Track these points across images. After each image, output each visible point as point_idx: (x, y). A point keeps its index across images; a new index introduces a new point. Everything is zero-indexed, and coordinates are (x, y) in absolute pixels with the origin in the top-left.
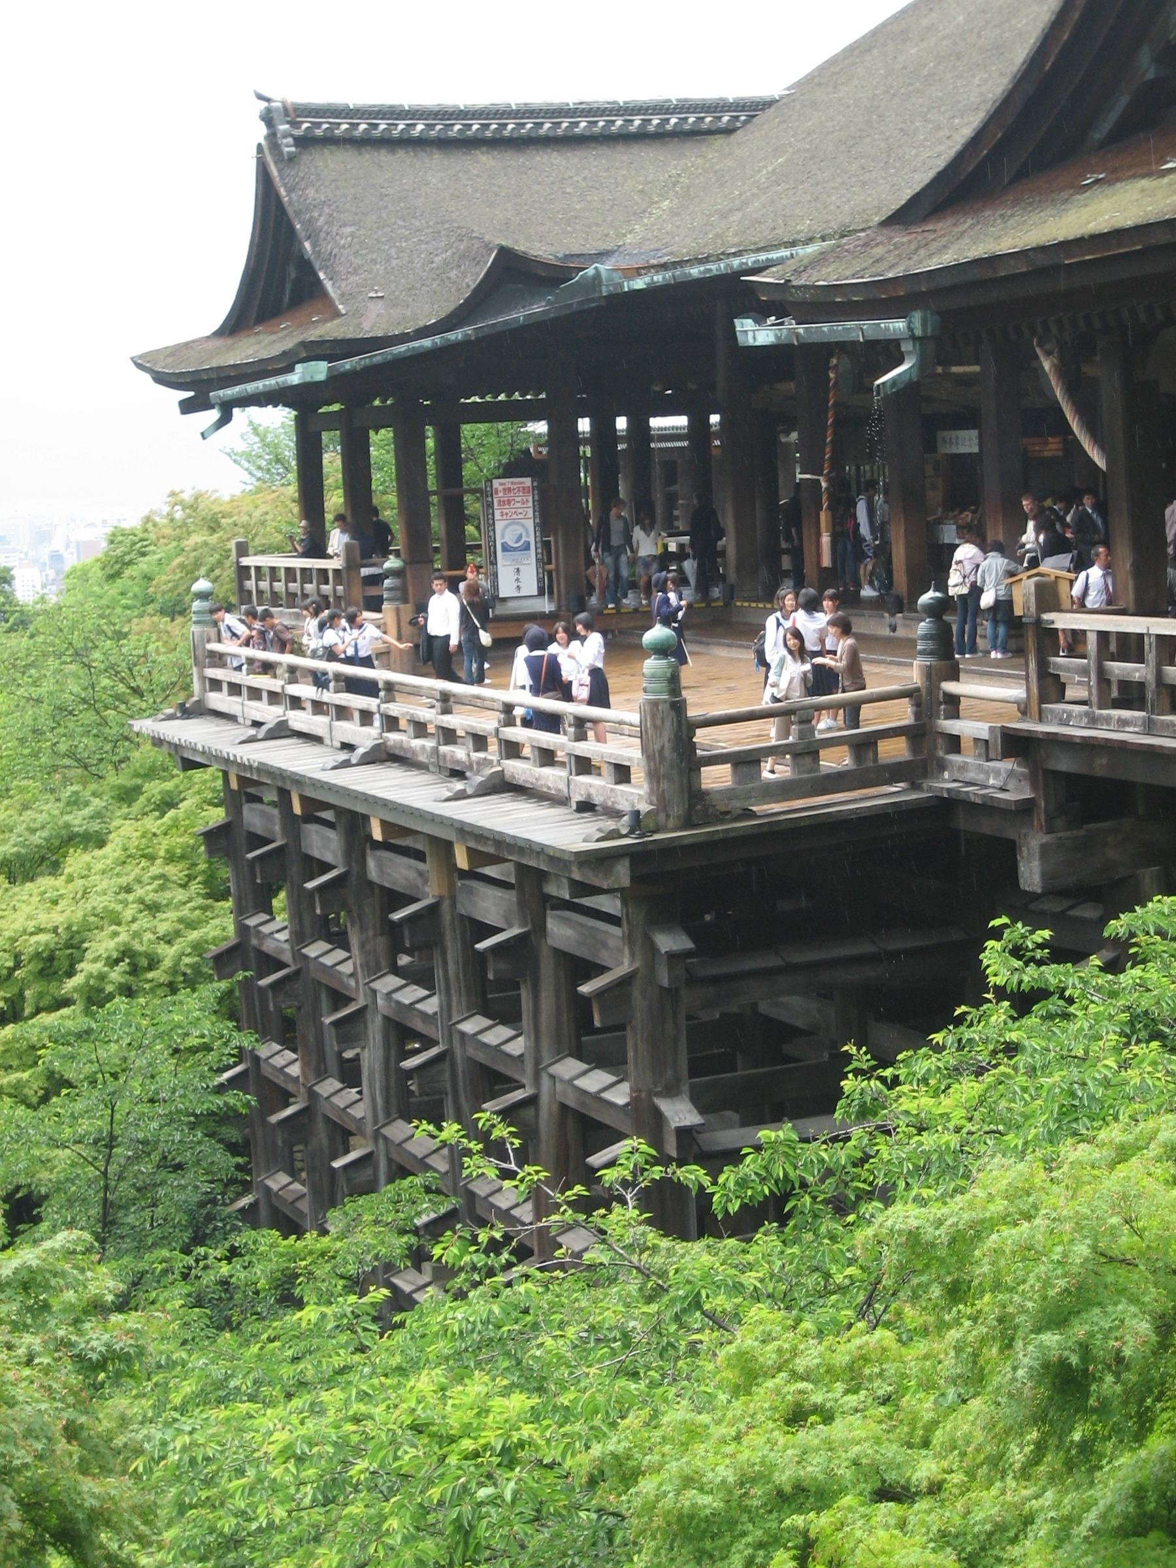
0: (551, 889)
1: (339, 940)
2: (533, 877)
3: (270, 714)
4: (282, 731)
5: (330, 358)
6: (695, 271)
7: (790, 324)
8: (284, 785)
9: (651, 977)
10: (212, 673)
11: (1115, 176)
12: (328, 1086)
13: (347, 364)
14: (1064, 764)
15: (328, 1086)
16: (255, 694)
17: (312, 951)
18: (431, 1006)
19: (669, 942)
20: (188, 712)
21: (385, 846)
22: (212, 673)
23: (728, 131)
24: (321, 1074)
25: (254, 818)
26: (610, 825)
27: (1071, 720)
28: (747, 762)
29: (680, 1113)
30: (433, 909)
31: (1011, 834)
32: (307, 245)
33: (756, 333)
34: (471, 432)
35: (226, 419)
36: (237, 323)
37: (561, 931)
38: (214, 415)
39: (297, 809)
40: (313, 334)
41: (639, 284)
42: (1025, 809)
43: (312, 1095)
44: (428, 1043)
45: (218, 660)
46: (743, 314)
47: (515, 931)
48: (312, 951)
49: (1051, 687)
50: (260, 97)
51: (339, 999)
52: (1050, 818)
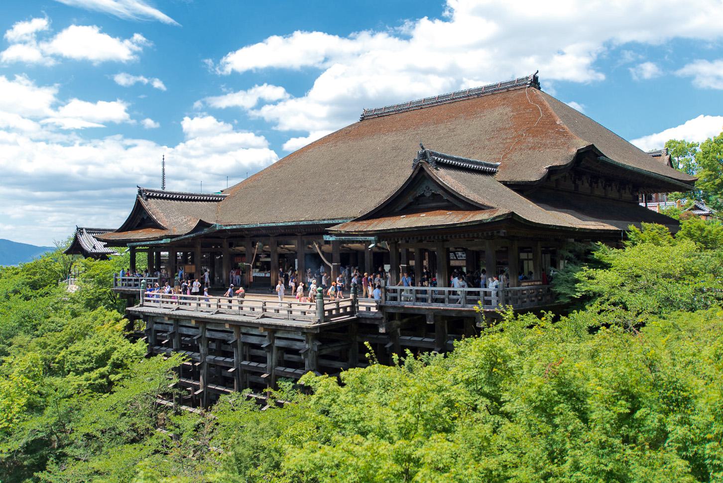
0: (278, 335)
3: (175, 306)
4: (178, 309)
5: (171, 238)
13: (174, 240)
14: (391, 311)
23: (221, 200)
28: (330, 311)
30: (236, 341)
31: (377, 323)
32: (154, 216)
33: (327, 238)
37: (278, 343)
41: (228, 228)
42: (382, 318)
45: (148, 296)
50: (138, 187)
52: (386, 319)
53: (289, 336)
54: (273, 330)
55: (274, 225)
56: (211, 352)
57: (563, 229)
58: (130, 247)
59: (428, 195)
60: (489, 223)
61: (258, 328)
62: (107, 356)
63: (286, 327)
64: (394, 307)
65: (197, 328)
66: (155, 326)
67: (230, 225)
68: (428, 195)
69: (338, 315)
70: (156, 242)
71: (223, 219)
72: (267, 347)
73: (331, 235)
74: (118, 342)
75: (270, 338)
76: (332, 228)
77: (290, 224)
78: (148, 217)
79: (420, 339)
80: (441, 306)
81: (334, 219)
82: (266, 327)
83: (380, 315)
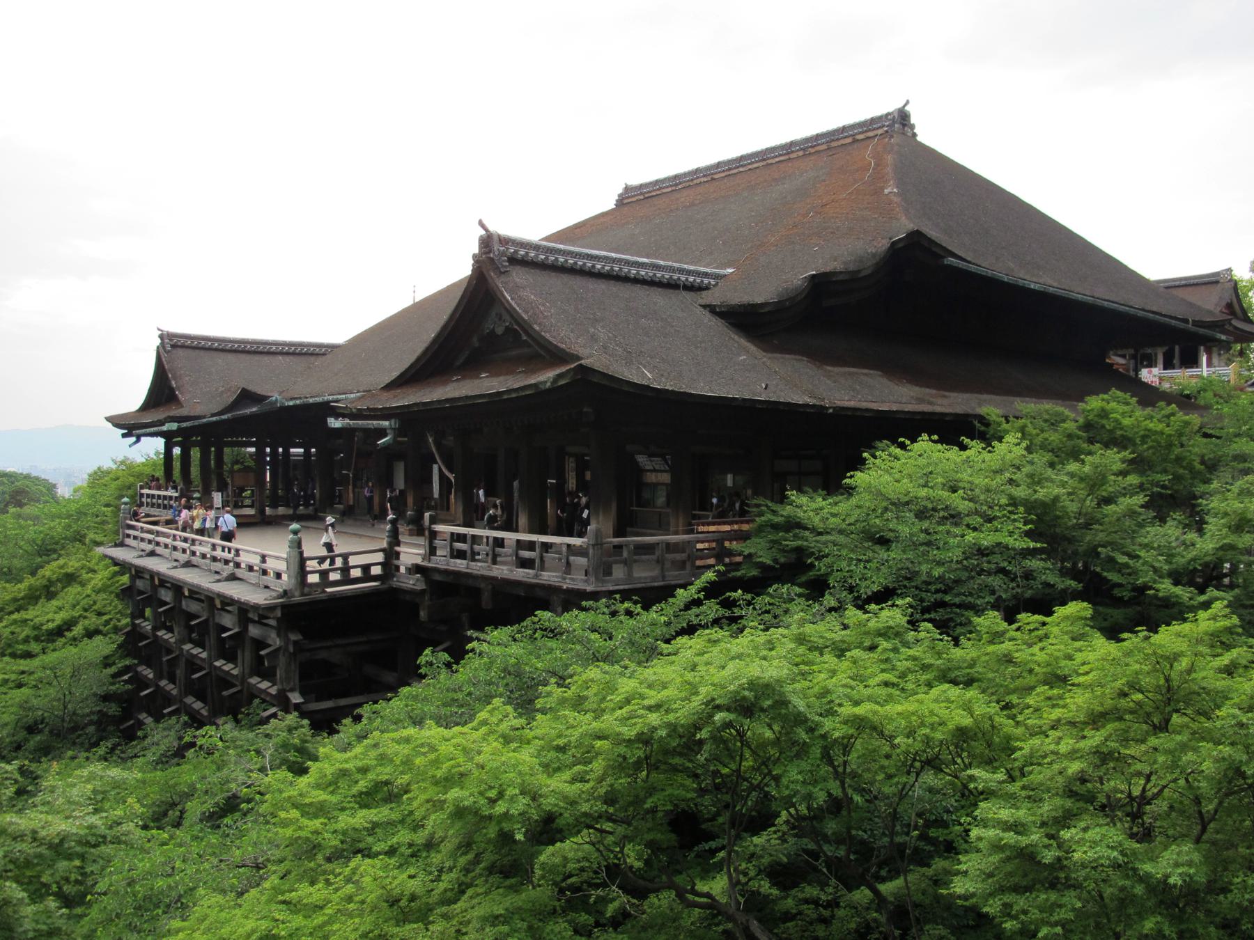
0: (251, 615)
1: (170, 630)
2: (245, 612)
4: (152, 554)
6: (311, 401)
7: (347, 421)
8: (153, 574)
9: (286, 649)
10: (128, 532)
11: (464, 378)
12: (163, 683)
13: (184, 425)
14: (437, 577)
16: (142, 540)
17: (159, 633)
18: (204, 655)
19: (294, 637)
20: (116, 545)
21: (190, 597)
22: (128, 532)
23: (324, 354)
24: (161, 678)
25: (140, 584)
26: (275, 594)
27: (442, 560)
29: (296, 698)
30: (206, 621)
34: (227, 450)
35: (138, 440)
36: (146, 407)
37: (254, 631)
38: (134, 439)
39: (157, 582)
40: (172, 413)
41: (291, 403)
42: (423, 592)
43: (157, 686)
44: (201, 669)
45: (132, 527)
46: (331, 416)
47: (236, 630)
48: (159, 633)
49: (432, 551)
51: (169, 651)
57: (781, 407)
59: (500, 331)
60: (549, 391)
68: (500, 331)
69: (346, 580)
71: (285, 389)
73: (344, 416)
74: (95, 607)
80: (504, 571)
83: (421, 586)
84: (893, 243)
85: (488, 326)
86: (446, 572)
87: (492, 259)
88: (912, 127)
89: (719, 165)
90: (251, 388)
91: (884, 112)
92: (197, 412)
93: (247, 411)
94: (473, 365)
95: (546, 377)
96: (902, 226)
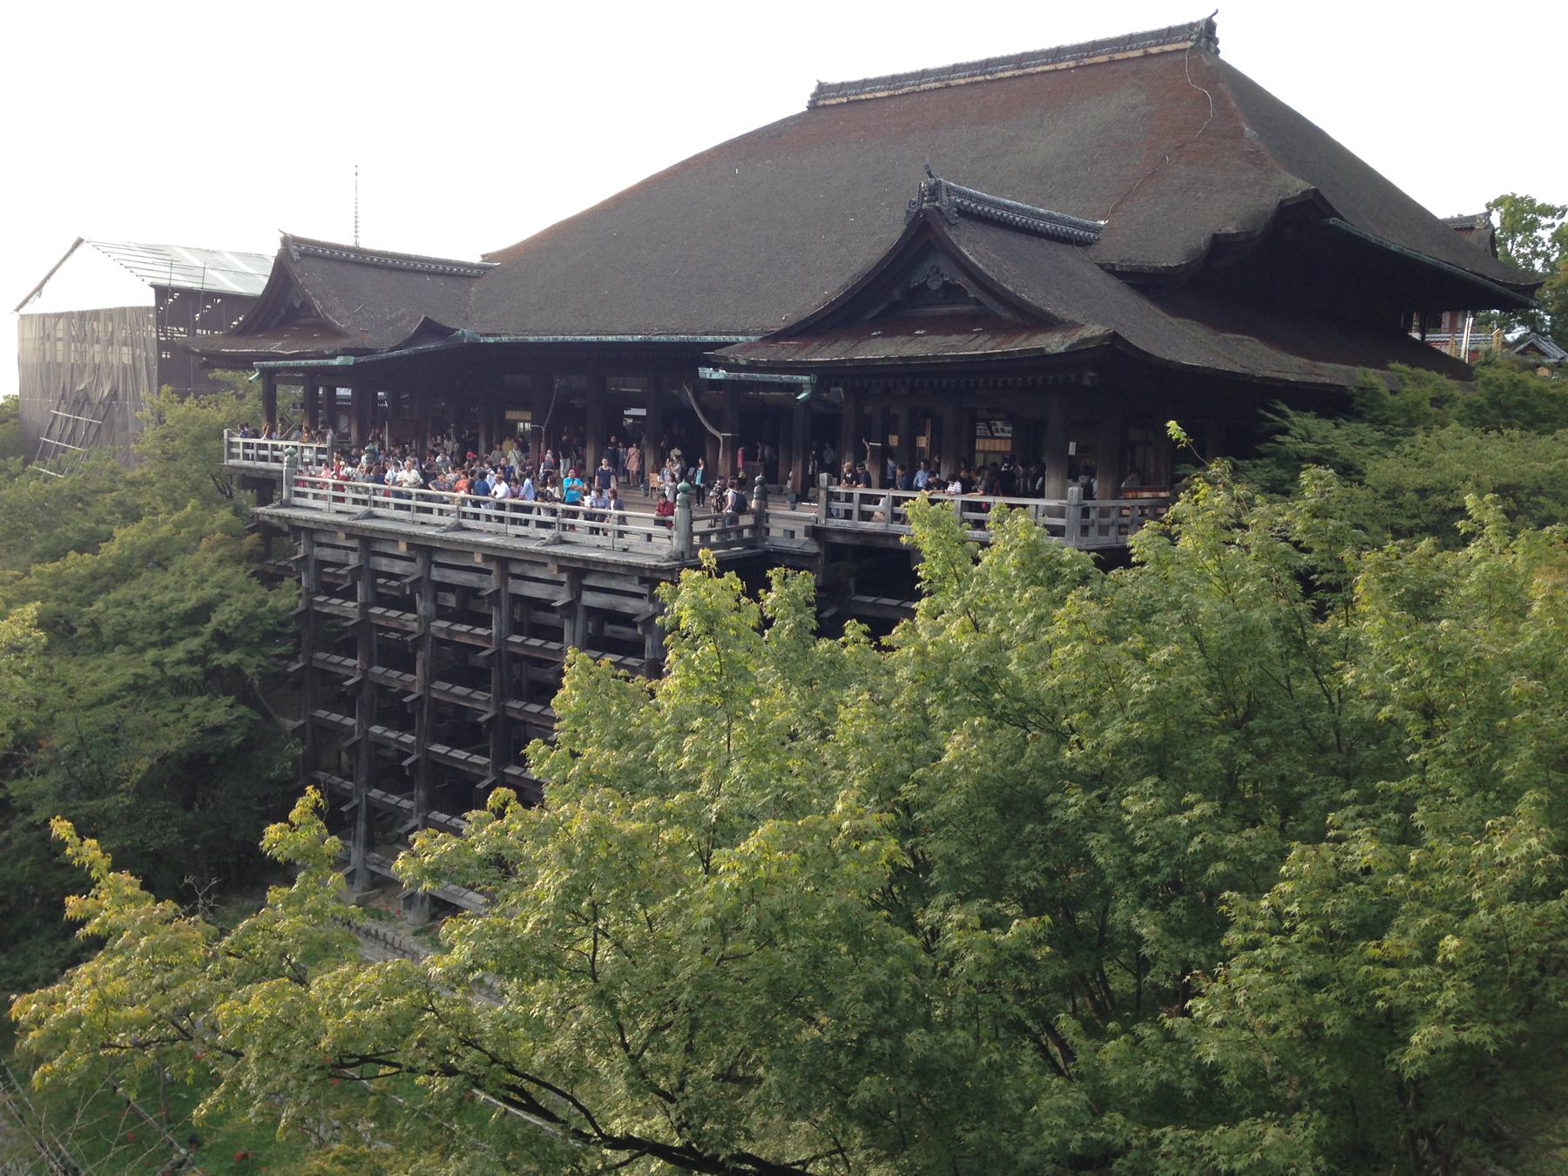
0: (589, 582)
3: (360, 509)
4: (370, 516)
6: (531, 339)
13: (361, 359)
14: (839, 539)
15: (379, 670)
30: (497, 592)
33: (707, 373)
37: (590, 599)
41: (491, 340)
53: (614, 584)
54: (579, 572)
55: (594, 338)
56: (442, 612)
58: (263, 370)
60: (1060, 354)
61: (545, 565)
62: (202, 612)
63: (605, 564)
64: (844, 532)
65: (413, 560)
66: (316, 549)
67: (494, 335)
70: (322, 362)
72: (562, 607)
73: (716, 367)
75: (572, 589)
76: (719, 352)
77: (629, 338)
78: (303, 304)
79: (895, 602)
81: (728, 334)
82: (565, 563)
84: (1282, 202)
85: (917, 280)
86: (862, 534)
87: (938, 209)
88: (1216, 41)
89: (956, 69)
90: (437, 320)
91: (1186, 21)
92: (369, 341)
93: (432, 346)
94: (895, 321)
95: (1054, 343)
96: (1297, 185)
